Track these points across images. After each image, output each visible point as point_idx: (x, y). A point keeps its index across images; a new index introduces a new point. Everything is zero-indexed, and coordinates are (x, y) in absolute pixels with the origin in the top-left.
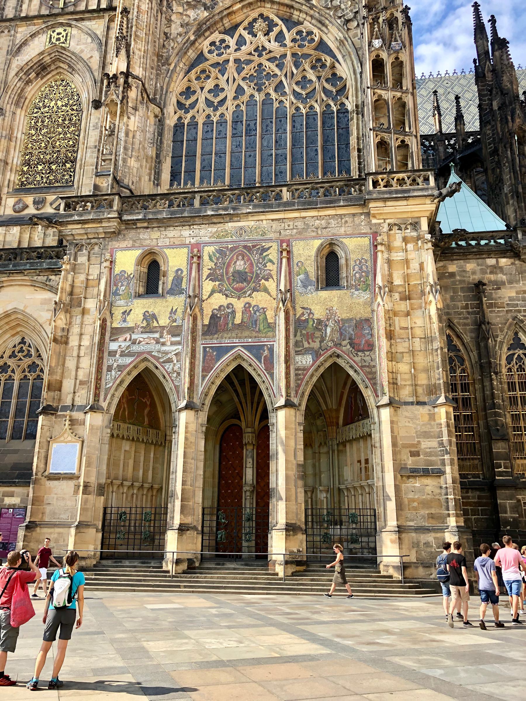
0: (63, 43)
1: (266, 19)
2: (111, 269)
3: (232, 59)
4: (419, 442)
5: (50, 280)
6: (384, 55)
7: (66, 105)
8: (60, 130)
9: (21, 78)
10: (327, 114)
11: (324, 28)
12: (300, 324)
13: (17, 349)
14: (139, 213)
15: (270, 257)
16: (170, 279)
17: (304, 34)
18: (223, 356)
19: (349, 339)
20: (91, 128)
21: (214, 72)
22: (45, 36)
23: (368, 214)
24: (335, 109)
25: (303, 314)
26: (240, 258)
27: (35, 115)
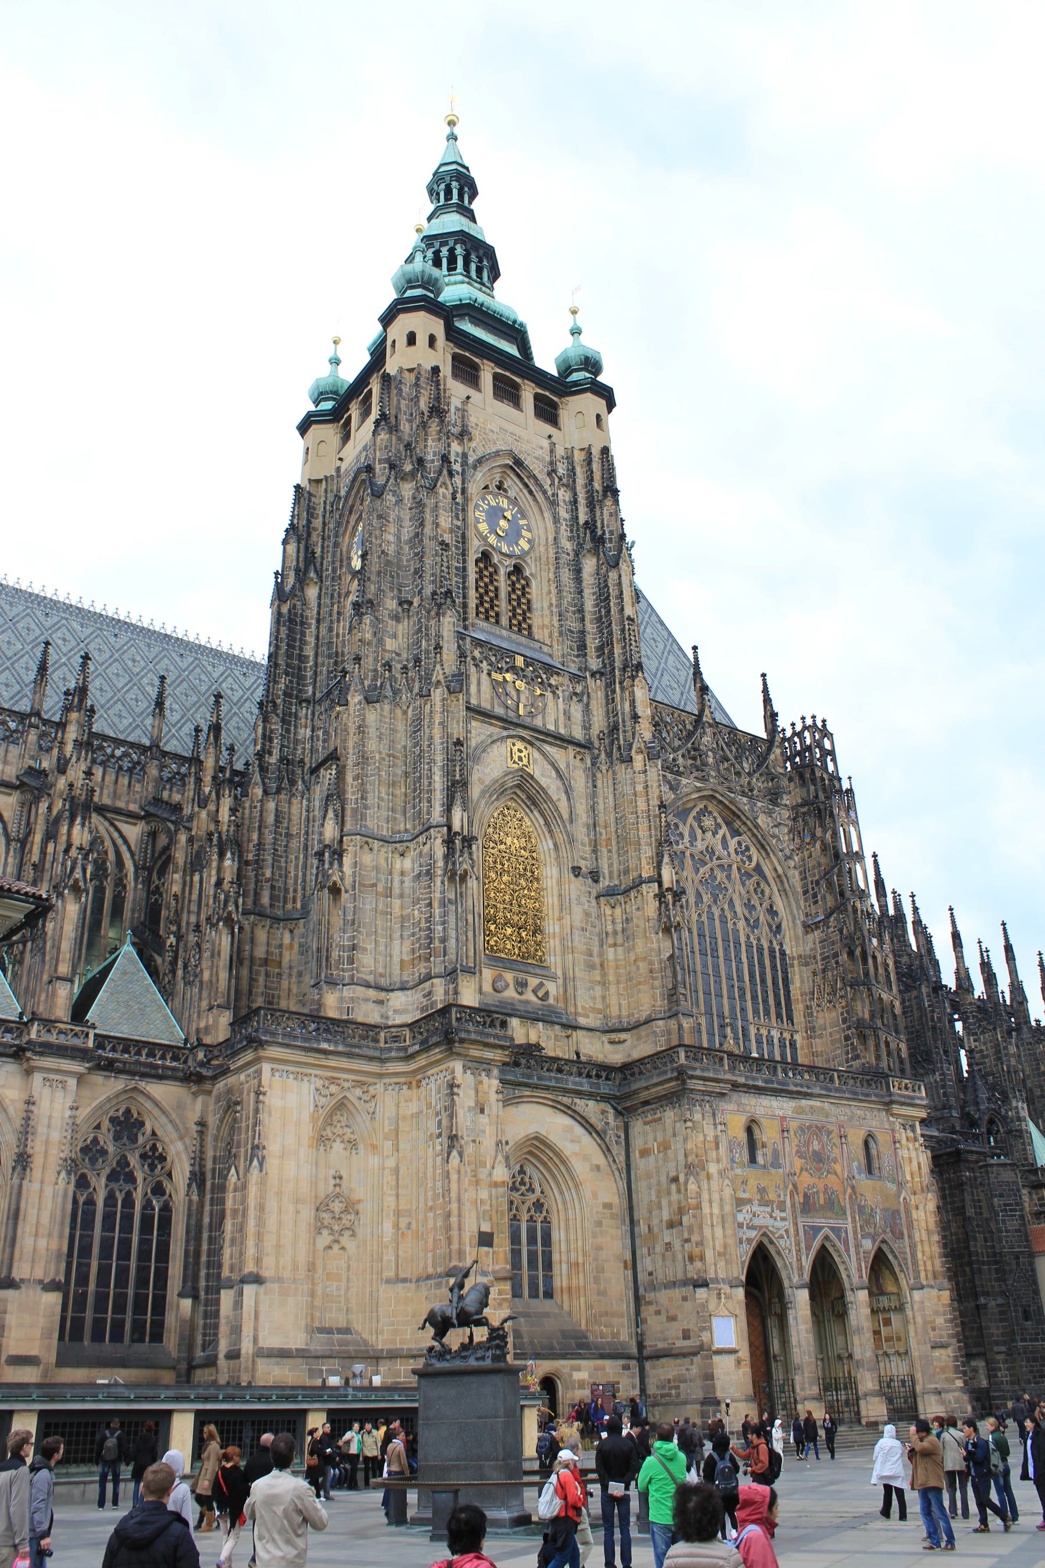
7: (525, 849)
8: (523, 882)
10: (772, 951)
12: (861, 1209)
16: (768, 1151)
23: (887, 1111)
24: (777, 948)
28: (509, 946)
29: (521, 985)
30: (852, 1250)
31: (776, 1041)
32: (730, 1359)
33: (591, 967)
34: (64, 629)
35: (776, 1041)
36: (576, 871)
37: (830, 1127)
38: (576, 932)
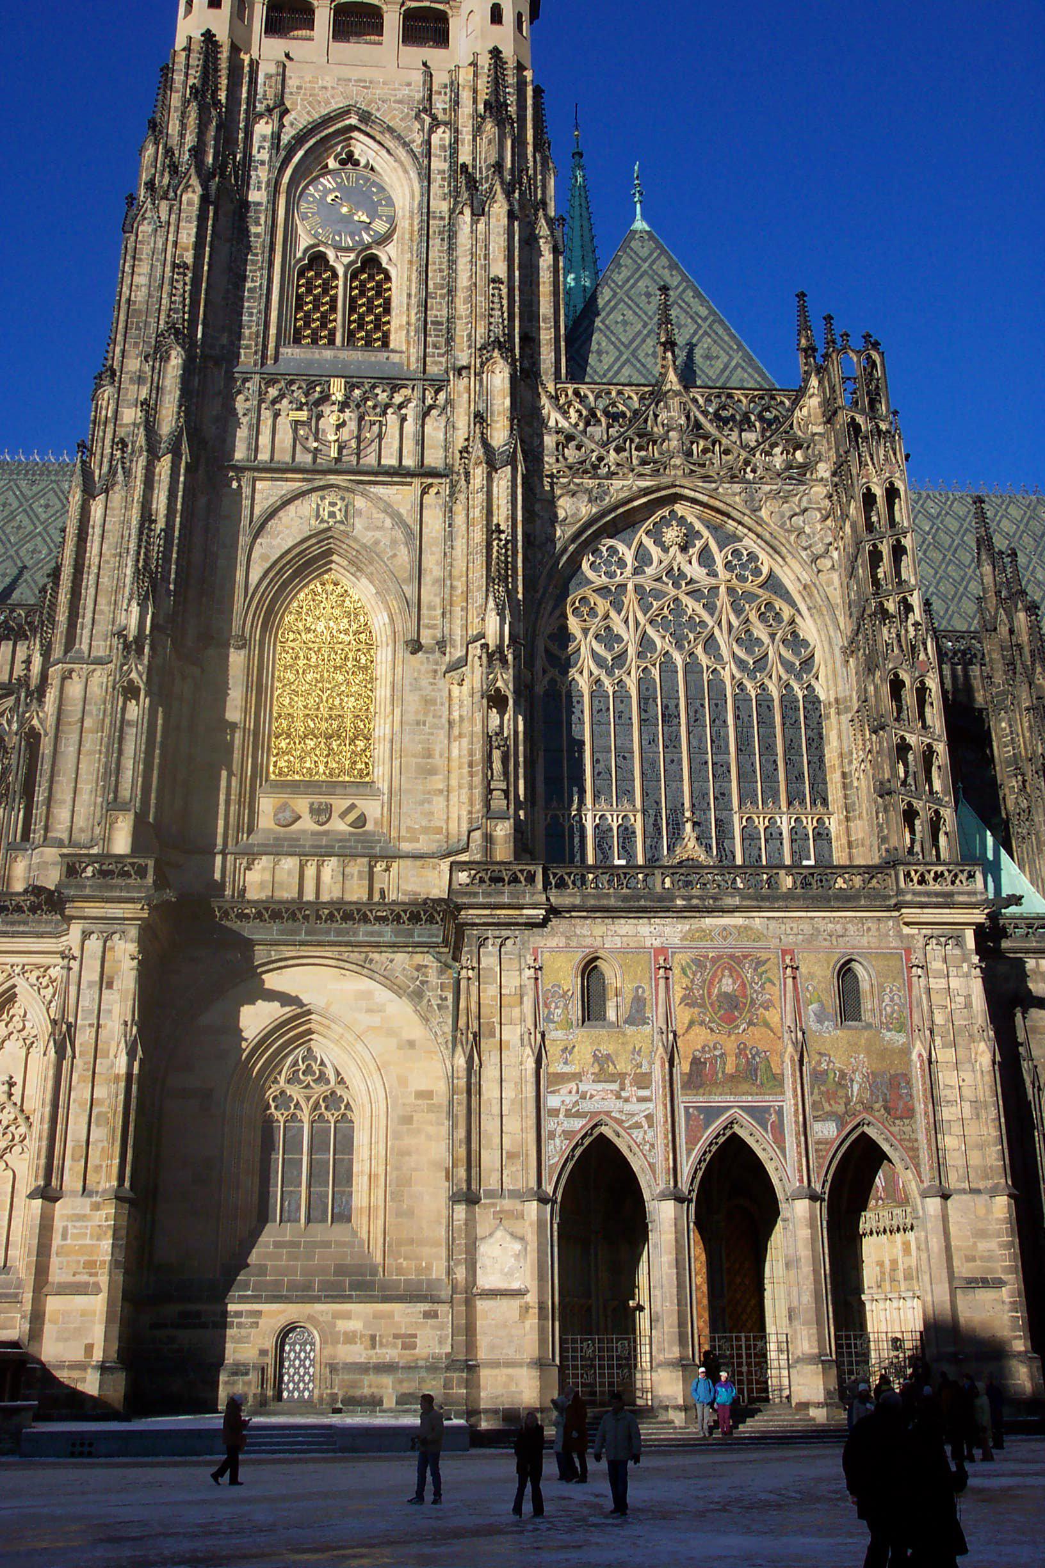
0: (341, 522)
1: (682, 521)
2: (536, 979)
3: (630, 587)
4: (975, 1243)
5: (371, 961)
6: (905, 676)
7: (346, 632)
8: (340, 678)
9: (272, 580)
10: (788, 702)
11: (776, 556)
12: (819, 1077)
13: (303, 1067)
14: (573, 895)
15: (769, 974)
16: (629, 1000)
17: (745, 558)
18: (714, 1122)
19: (884, 1100)
20: (407, 688)
21: (602, 605)
22: (306, 505)
24: (800, 695)
25: (819, 1063)
26: (727, 973)
27: (292, 644)
28: (308, 765)
29: (321, 813)
30: (790, 1141)
31: (786, 834)
32: (508, 1308)
33: (432, 771)
34: (51, 494)
35: (786, 834)
36: (416, 647)
37: (764, 956)
38: (406, 728)
